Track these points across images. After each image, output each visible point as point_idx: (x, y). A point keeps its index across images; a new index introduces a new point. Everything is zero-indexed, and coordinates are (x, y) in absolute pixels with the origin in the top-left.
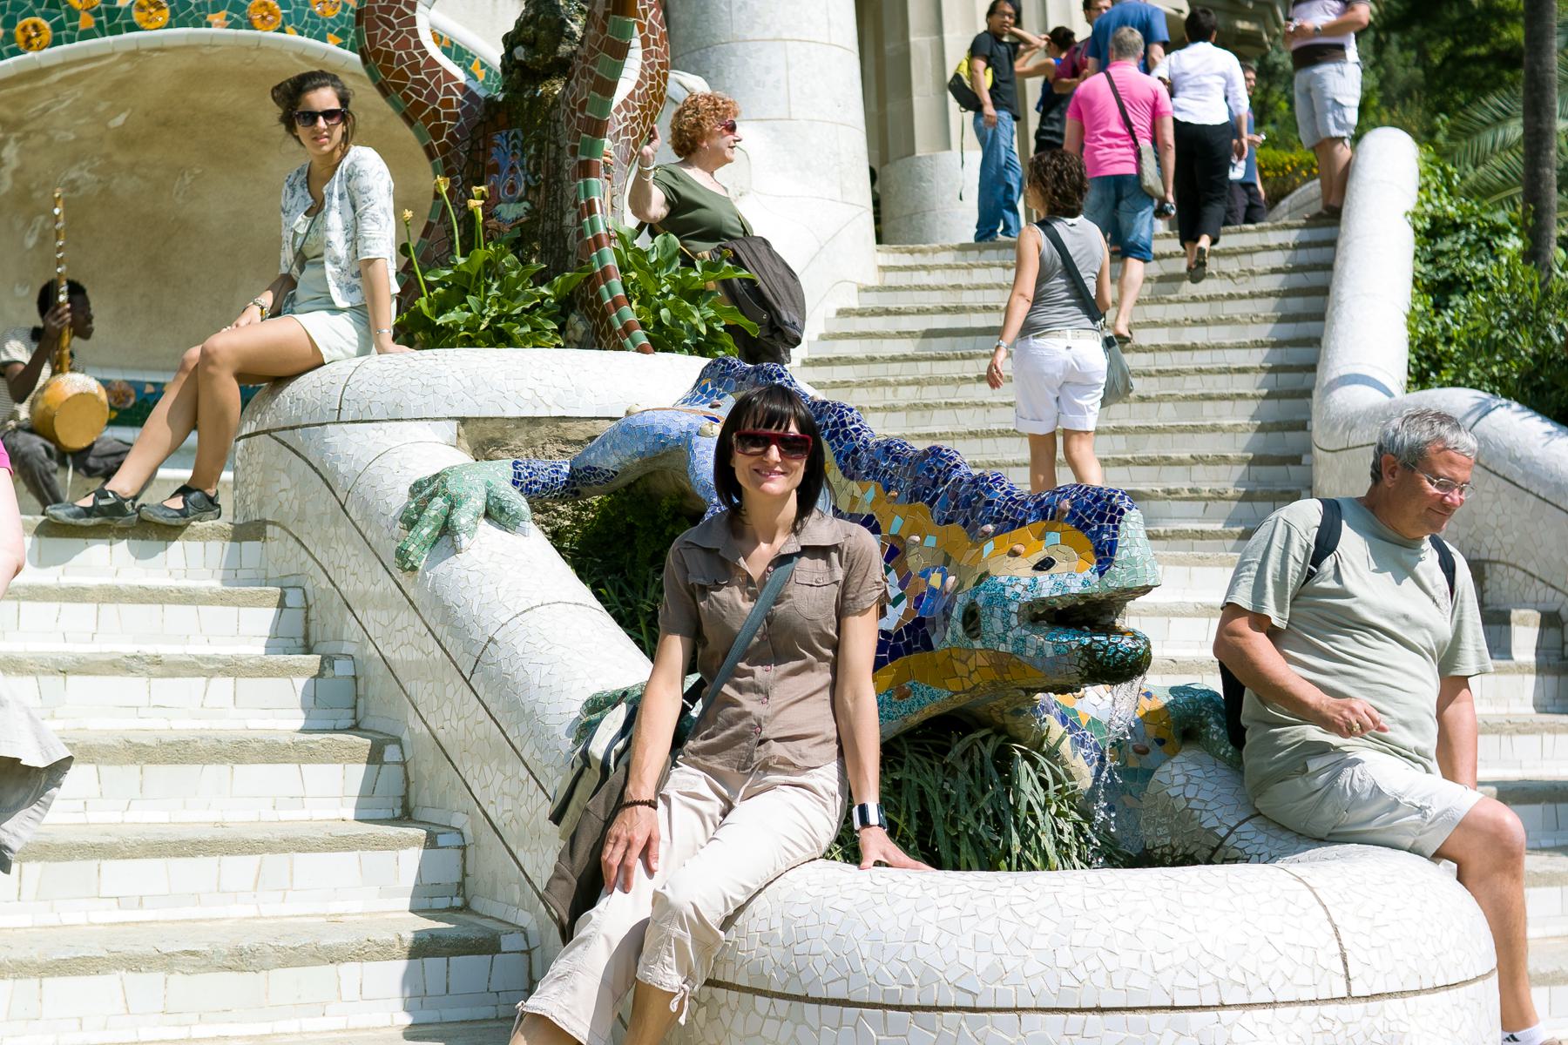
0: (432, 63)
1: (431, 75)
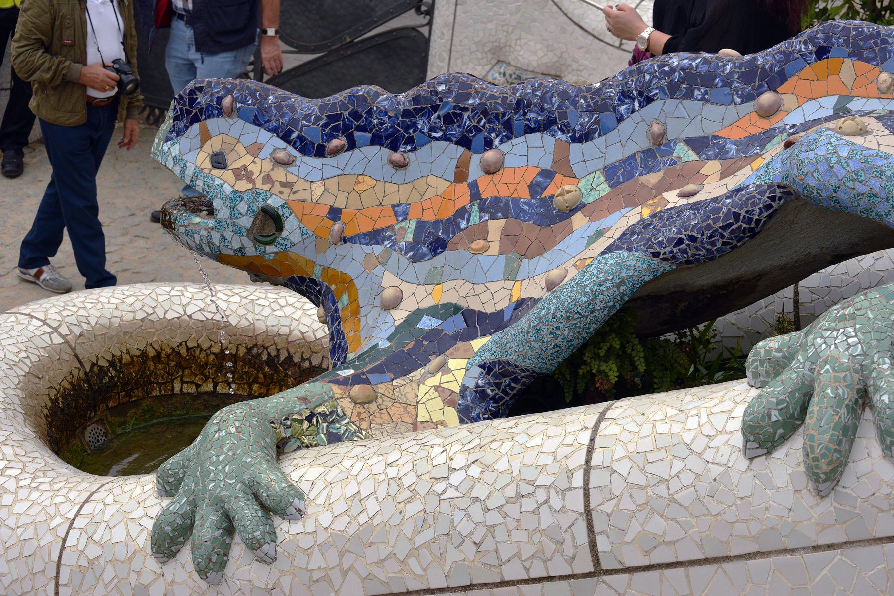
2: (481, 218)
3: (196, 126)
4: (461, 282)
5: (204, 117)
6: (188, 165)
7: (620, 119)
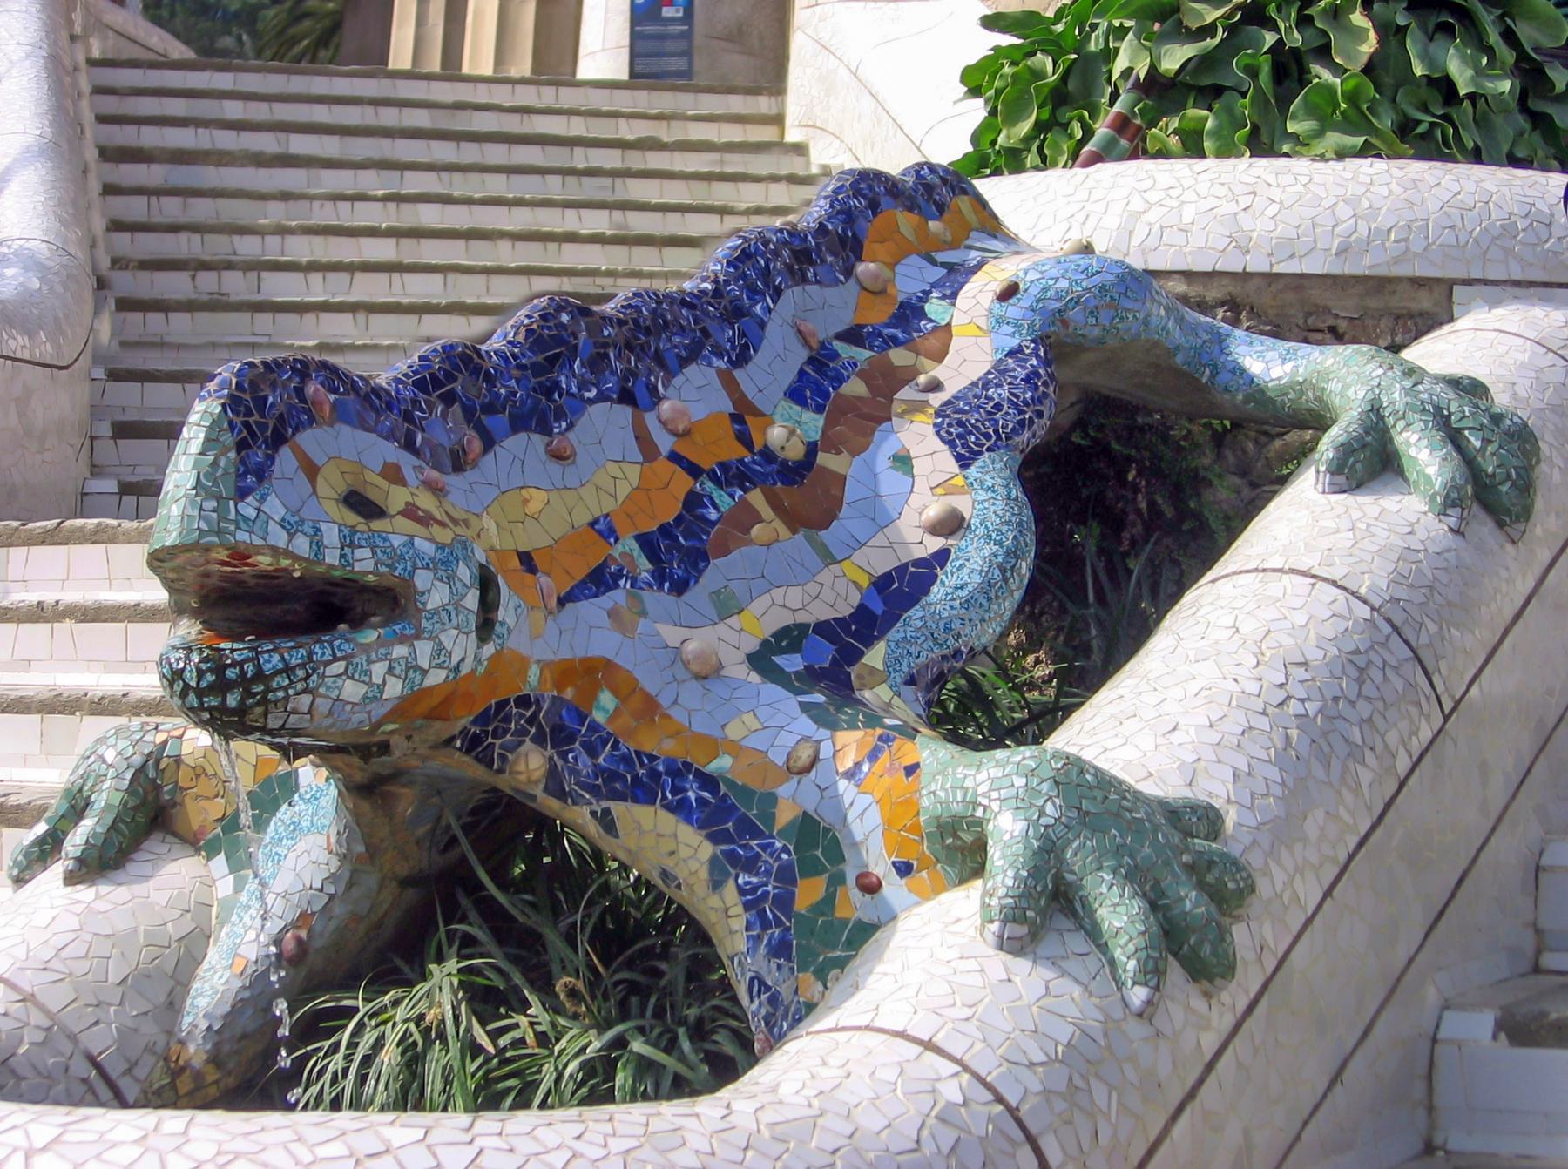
2: (732, 496)
3: (285, 452)
4: (775, 592)
5: (290, 430)
6: (323, 526)
7: (762, 325)
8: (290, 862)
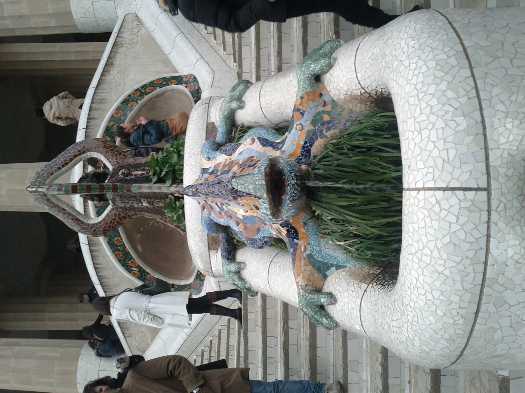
0: (104, 219)
1: (108, 220)
8: (326, 251)
